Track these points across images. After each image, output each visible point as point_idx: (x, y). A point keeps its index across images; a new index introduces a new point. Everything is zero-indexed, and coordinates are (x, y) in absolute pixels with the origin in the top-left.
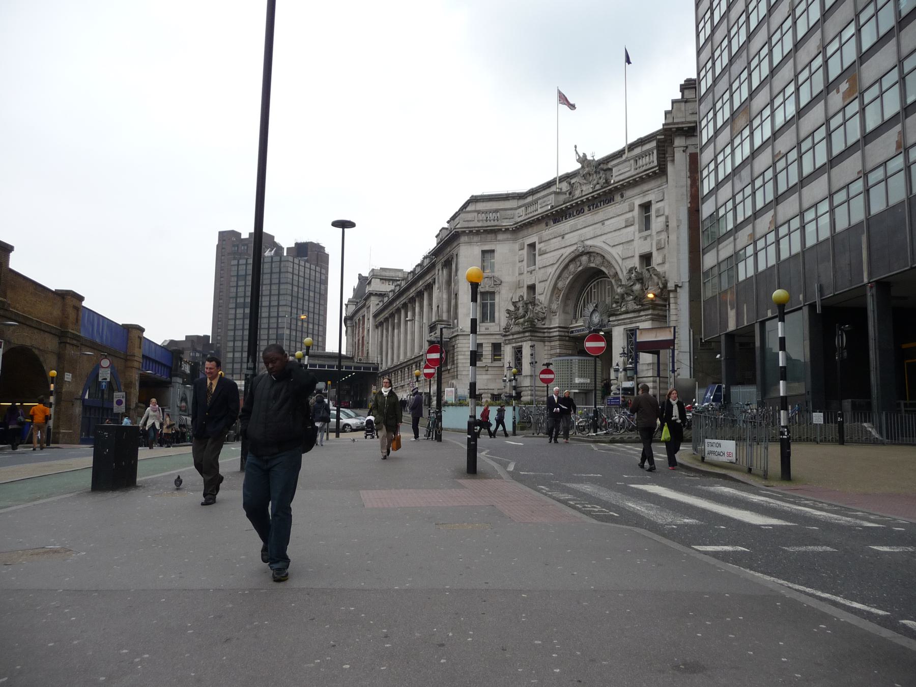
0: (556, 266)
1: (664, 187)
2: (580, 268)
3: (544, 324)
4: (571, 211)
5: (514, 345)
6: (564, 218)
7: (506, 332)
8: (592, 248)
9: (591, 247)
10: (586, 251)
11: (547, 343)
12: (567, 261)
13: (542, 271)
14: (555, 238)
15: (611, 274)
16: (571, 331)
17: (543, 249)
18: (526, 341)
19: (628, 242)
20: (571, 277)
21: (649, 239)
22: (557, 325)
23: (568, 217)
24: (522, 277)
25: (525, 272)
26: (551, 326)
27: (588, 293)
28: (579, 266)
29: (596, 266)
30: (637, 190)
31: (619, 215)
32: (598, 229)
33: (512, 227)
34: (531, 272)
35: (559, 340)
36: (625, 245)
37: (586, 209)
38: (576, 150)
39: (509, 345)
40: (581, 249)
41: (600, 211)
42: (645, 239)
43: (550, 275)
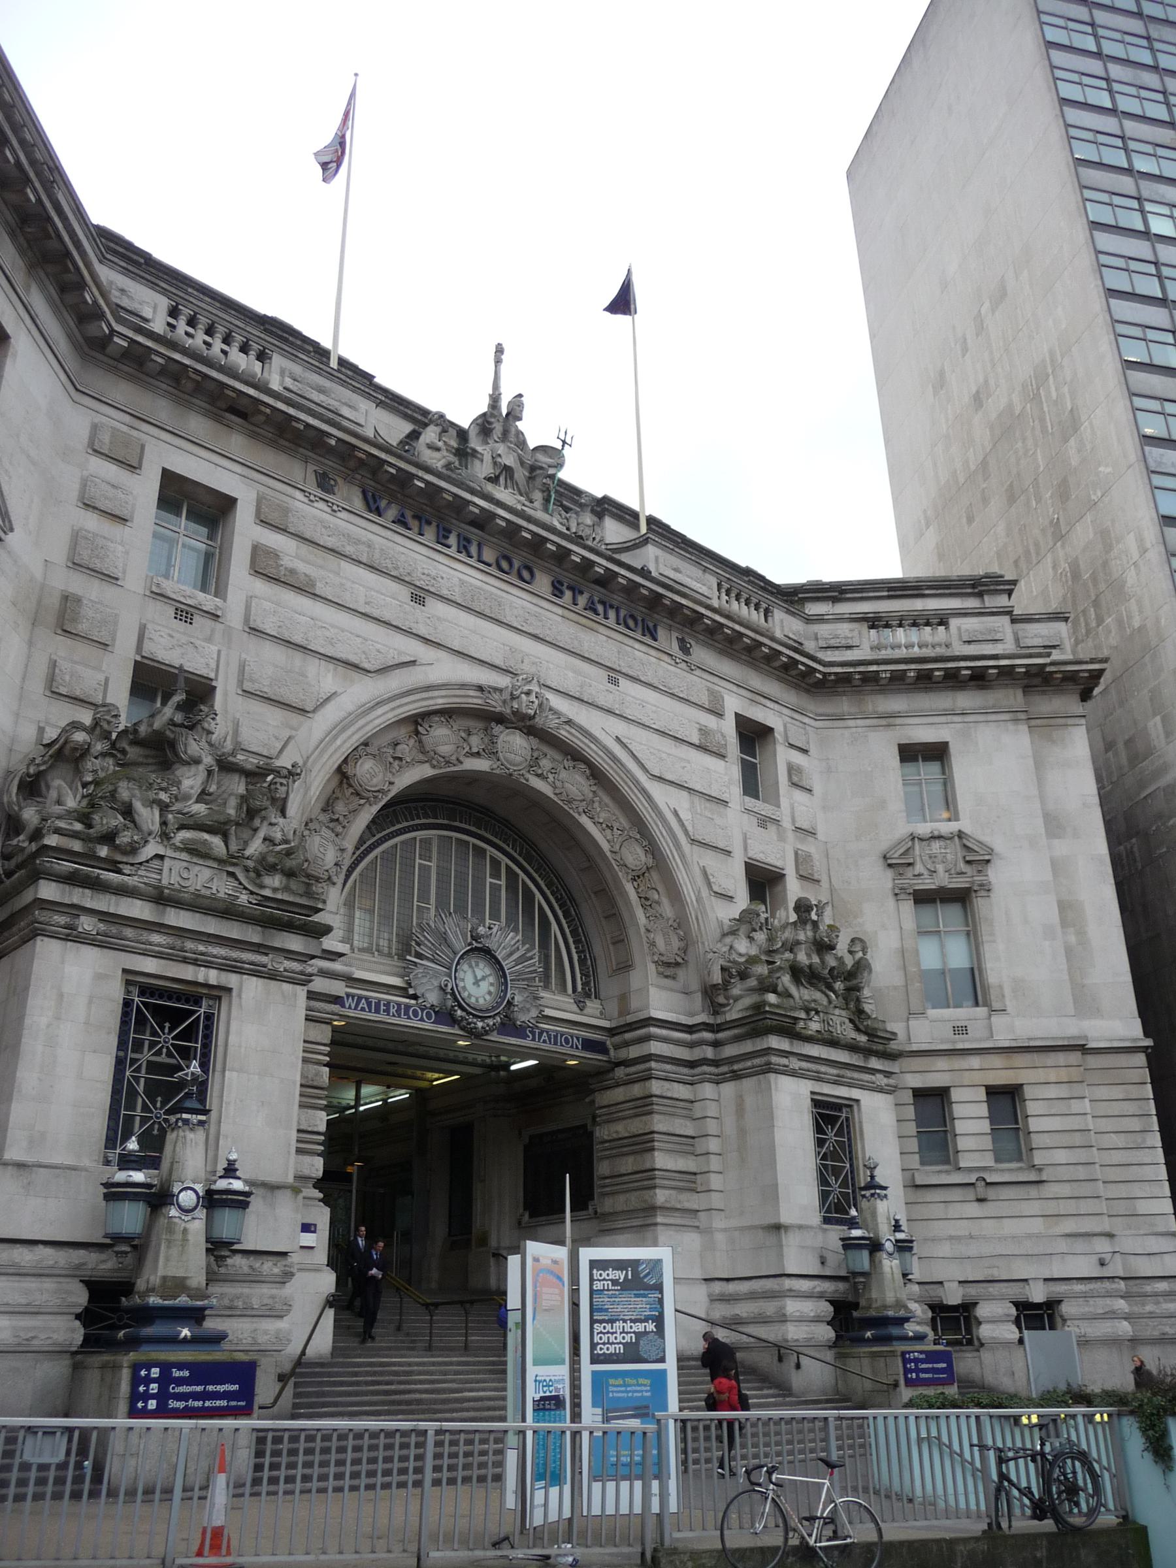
0: (362, 691)
1: (806, 720)
2: (482, 765)
4: (474, 533)
5: (150, 965)
6: (430, 534)
7: (90, 857)
8: (567, 727)
9: (569, 722)
10: (539, 721)
12: (439, 701)
13: (273, 654)
14: (372, 567)
15: (630, 860)
17: (301, 567)
18: (273, 976)
19: (710, 798)
20: (426, 771)
21: (772, 828)
23: (452, 540)
24: (90, 590)
25: (135, 580)
27: (389, 856)
30: (727, 667)
31: (673, 695)
32: (595, 684)
33: (118, 328)
34: (185, 613)
36: (696, 799)
37: (543, 582)
38: (498, 362)
39: (90, 954)
40: (526, 705)
41: (602, 629)
42: (764, 822)
43: (328, 699)
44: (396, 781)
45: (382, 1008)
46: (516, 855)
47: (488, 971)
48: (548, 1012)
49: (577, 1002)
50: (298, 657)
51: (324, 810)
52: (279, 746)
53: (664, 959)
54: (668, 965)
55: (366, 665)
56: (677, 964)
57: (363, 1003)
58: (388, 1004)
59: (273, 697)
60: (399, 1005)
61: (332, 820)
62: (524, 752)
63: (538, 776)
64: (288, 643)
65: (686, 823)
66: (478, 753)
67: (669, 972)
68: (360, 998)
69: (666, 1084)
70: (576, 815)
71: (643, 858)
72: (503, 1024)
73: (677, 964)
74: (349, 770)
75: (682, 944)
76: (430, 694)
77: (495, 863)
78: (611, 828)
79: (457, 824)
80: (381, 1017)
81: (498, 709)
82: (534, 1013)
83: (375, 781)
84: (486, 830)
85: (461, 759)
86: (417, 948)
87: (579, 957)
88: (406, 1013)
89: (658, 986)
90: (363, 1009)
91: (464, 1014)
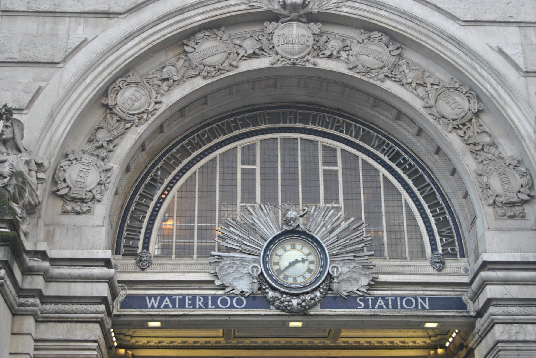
3: (26, 234)
11: (29, 323)
16: (128, 297)
20: (200, 82)
22: (108, 254)
26: (53, 253)
28: (254, 55)
29: (351, 73)
35: (101, 322)
43: (78, 48)
44: (164, 99)
45: (187, 302)
46: (352, 139)
47: (306, 250)
48: (383, 278)
49: (433, 263)
50: (49, 22)
51: (90, 141)
52: (28, 98)
53: (503, 199)
54: (512, 204)
55: (117, 9)
56: (524, 202)
57: (167, 301)
58: (193, 299)
59: (22, 60)
60: (206, 297)
61: (98, 148)
62: (304, 40)
63: (330, 57)
64: (38, 13)
65: (514, 58)
66: (254, 53)
67: (517, 210)
68: (163, 297)
69: (515, 327)
70: (378, 83)
71: (466, 105)
72: (324, 297)
73: (524, 202)
74: (110, 102)
75: (525, 181)
76: (186, 15)
77: (330, 151)
78: (424, 85)
79: (281, 125)
80: (188, 310)
81: (265, 8)
82: (365, 281)
83: (137, 104)
84: (314, 123)
85: (235, 63)
86: (223, 243)
87: (437, 221)
88: (214, 303)
89: (497, 229)
90: (167, 307)
91: (277, 294)
